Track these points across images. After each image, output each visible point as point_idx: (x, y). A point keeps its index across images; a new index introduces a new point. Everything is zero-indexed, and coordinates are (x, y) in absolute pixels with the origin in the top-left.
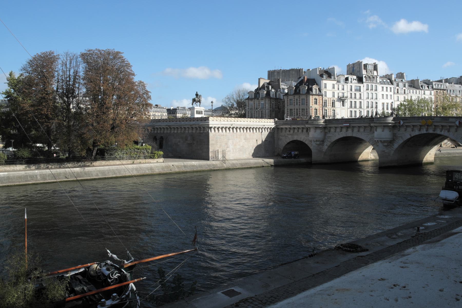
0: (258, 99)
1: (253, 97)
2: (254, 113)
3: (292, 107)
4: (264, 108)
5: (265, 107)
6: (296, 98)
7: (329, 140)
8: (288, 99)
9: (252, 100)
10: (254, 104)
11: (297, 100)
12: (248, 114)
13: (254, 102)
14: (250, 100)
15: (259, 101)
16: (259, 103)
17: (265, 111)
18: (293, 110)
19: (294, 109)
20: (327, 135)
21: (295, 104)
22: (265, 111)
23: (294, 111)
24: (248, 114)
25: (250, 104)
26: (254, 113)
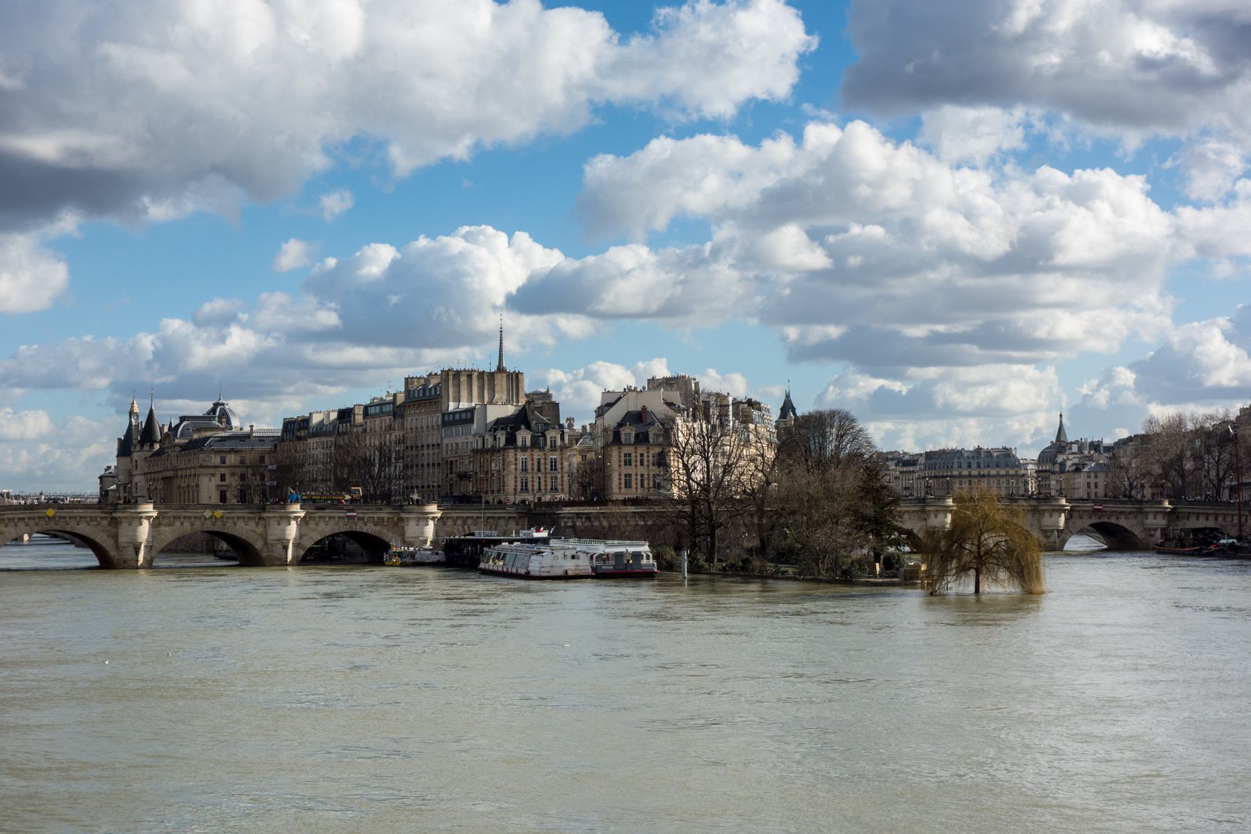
0: (542, 449)
1: (528, 443)
2: (533, 481)
4: (560, 471)
5: (562, 468)
6: (639, 452)
8: (620, 452)
9: (526, 451)
10: (533, 459)
11: (642, 455)
12: (516, 481)
13: (532, 455)
14: (519, 450)
15: (545, 454)
16: (545, 459)
17: (562, 477)
19: (636, 475)
21: (638, 464)
22: (562, 477)
23: (636, 479)
24: (516, 481)
26: (533, 481)
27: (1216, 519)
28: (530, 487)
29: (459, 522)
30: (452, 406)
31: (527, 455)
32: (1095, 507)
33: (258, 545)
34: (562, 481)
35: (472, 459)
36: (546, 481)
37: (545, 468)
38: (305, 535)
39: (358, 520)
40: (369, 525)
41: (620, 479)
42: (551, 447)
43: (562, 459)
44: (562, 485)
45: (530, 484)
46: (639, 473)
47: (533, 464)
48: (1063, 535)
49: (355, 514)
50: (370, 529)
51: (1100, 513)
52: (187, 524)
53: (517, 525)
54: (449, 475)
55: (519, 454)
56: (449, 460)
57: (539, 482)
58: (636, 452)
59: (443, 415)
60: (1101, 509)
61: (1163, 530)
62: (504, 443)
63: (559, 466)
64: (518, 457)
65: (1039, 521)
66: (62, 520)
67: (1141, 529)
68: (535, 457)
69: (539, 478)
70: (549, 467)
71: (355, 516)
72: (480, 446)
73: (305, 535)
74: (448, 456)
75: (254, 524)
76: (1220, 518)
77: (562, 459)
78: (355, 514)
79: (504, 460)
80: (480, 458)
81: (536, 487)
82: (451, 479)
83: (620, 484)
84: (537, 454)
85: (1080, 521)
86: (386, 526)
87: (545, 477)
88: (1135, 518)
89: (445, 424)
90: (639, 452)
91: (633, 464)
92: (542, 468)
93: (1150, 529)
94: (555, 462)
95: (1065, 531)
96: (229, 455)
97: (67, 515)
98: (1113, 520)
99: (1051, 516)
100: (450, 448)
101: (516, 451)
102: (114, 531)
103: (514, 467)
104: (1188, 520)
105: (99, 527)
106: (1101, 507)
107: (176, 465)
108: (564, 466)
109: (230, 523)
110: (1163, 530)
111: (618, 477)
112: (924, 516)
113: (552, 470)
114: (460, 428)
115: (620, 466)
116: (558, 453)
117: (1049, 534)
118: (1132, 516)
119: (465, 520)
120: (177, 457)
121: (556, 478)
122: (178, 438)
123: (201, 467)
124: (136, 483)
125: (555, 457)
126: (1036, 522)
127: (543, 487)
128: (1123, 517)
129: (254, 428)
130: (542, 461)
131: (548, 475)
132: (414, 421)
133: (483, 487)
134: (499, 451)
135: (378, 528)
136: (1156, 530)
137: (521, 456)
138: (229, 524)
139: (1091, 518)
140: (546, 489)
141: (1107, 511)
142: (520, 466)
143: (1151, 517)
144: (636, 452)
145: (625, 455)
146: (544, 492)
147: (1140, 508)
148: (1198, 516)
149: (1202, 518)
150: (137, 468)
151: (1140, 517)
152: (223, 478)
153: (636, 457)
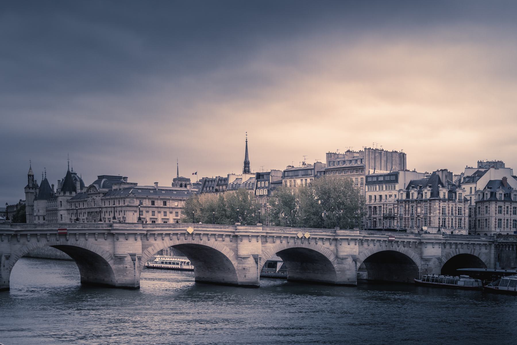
0: (454, 201)
1: (447, 197)
2: (449, 221)
3: (501, 216)
4: (463, 215)
5: (465, 214)
6: (506, 205)
8: (496, 205)
9: (445, 201)
10: (449, 207)
11: (507, 207)
13: (449, 204)
14: (441, 201)
15: (456, 204)
16: (456, 207)
17: (465, 219)
18: (503, 221)
19: (504, 220)
21: (506, 213)
22: (465, 219)
23: (504, 222)
25: (441, 207)
26: (449, 221)
28: (447, 225)
29: (453, 246)
30: (372, 172)
31: (446, 203)
33: (331, 258)
34: (465, 222)
35: (395, 206)
36: (456, 221)
37: (456, 213)
38: (362, 252)
39: (395, 242)
40: (400, 246)
41: (496, 222)
42: (459, 200)
43: (465, 208)
44: (465, 224)
45: (447, 223)
46: (506, 219)
47: (449, 210)
49: (394, 239)
50: (401, 249)
52: (284, 242)
53: (486, 249)
54: (372, 216)
55: (441, 203)
56: (372, 206)
57: (452, 222)
58: (505, 205)
59: (367, 177)
62: (430, 196)
63: (463, 212)
64: (441, 205)
66: (198, 236)
68: (450, 206)
69: (452, 219)
70: (457, 212)
71: (394, 240)
72: (404, 197)
73: (362, 252)
74: (372, 203)
75: (329, 244)
77: (465, 208)
78: (394, 239)
79: (430, 207)
80: (405, 205)
81: (450, 225)
82: (376, 218)
83: (496, 225)
84: (451, 204)
86: (410, 247)
87: (456, 219)
89: (368, 183)
90: (506, 205)
91: (503, 212)
92: (454, 212)
94: (461, 209)
96: (144, 200)
97: (202, 232)
100: (373, 198)
101: (440, 201)
102: (235, 245)
103: (438, 211)
105: (224, 243)
107: (100, 204)
108: (466, 212)
109: (313, 242)
111: (495, 220)
113: (459, 214)
114: (384, 186)
115: (496, 214)
116: (462, 204)
119: (456, 244)
120: (102, 200)
121: (461, 219)
122: (101, 188)
123: (128, 206)
124: (61, 215)
125: (461, 206)
127: (454, 225)
129: (159, 185)
130: (454, 209)
131: (457, 218)
132: (304, 181)
133: (408, 224)
134: (426, 201)
135: (406, 248)
137: (442, 204)
138: (313, 243)
140: (456, 227)
142: (441, 211)
144: (505, 205)
145: (499, 206)
146: (454, 228)
150: (61, 206)
152: (177, 213)
153: (504, 208)
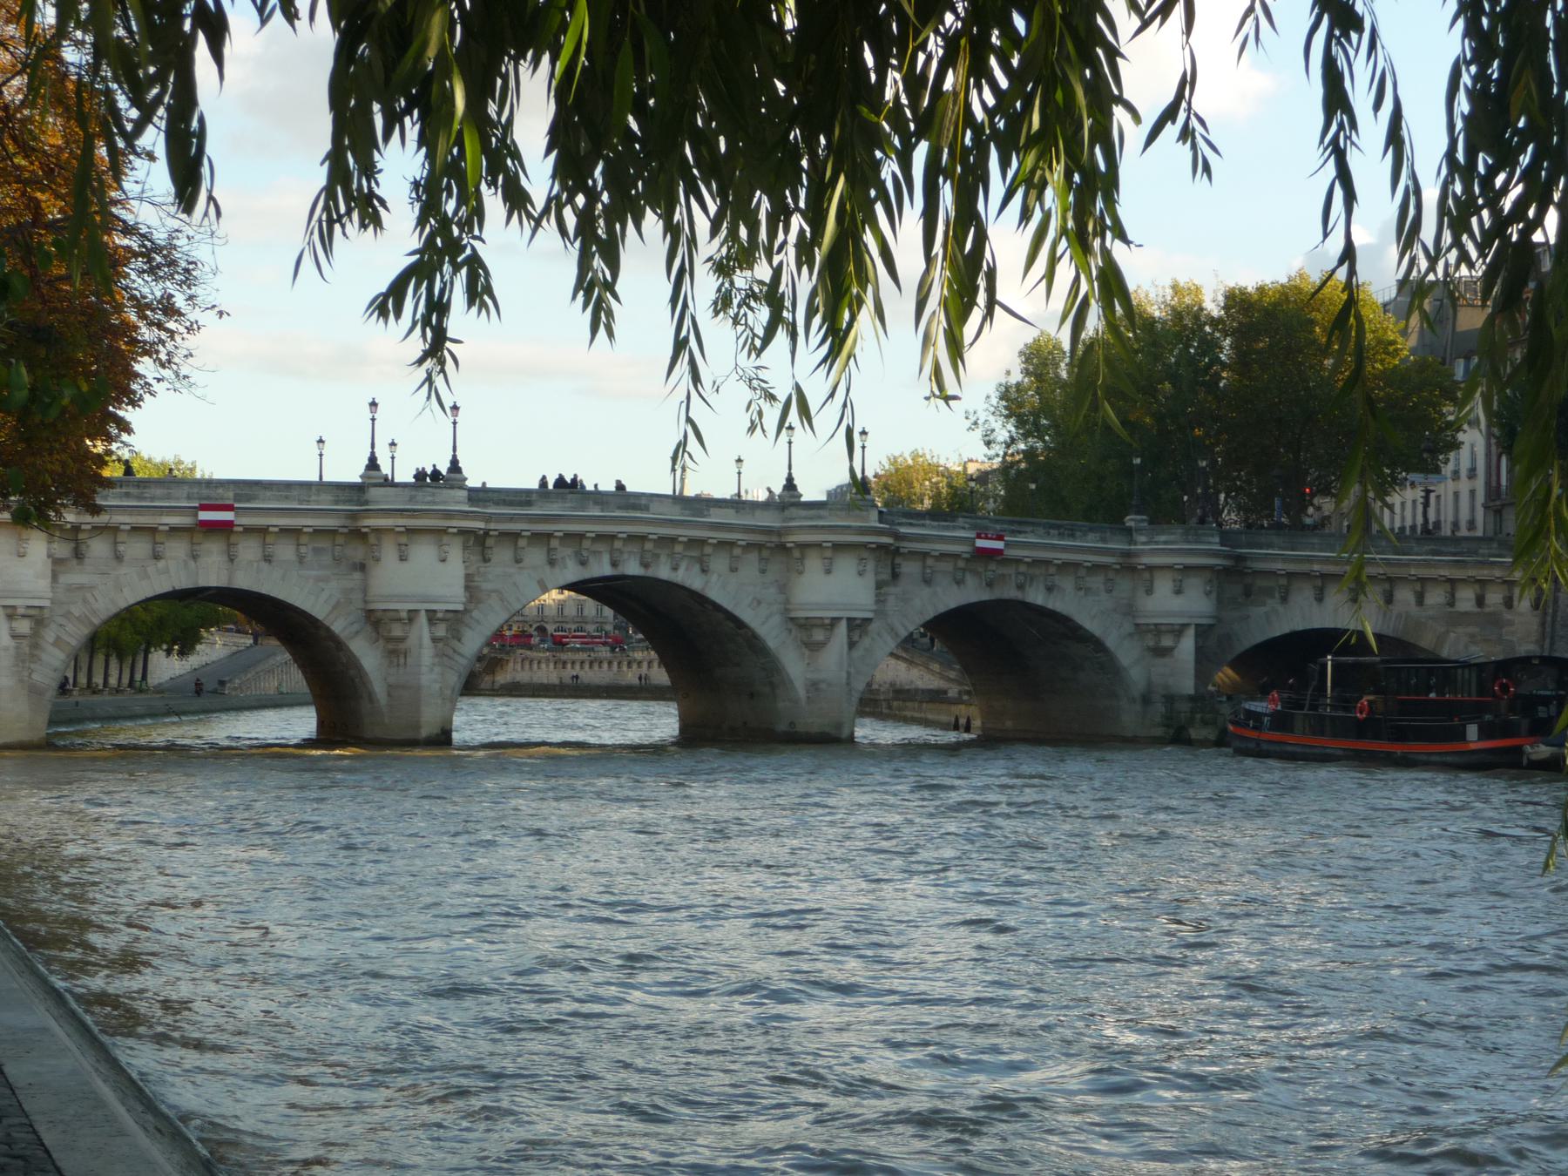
7: (77, 610)
20: (63, 579)
27: (1389, 599)
32: (980, 543)
48: (866, 641)
51: (992, 566)
60: (999, 552)
61: (1202, 632)
65: (783, 588)
67: (1128, 627)
76: (1405, 595)
85: (926, 591)
88: (1109, 591)
93: (1158, 630)
95: (873, 627)
98: (1036, 596)
99: (828, 572)
104: (1284, 599)
106: (999, 545)
110: (1202, 632)
112: (357, 552)
117: (819, 635)
118: (1096, 582)
126: (773, 590)
128: (1067, 583)
136: (1179, 631)
139: (959, 582)
141: (1018, 561)
143: (1163, 585)
147: (1127, 554)
148: (1322, 583)
149: (1336, 597)
151: (1124, 585)
